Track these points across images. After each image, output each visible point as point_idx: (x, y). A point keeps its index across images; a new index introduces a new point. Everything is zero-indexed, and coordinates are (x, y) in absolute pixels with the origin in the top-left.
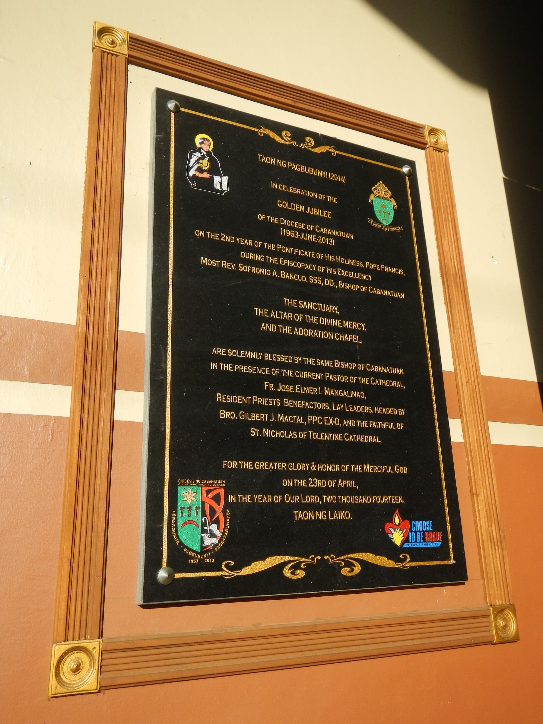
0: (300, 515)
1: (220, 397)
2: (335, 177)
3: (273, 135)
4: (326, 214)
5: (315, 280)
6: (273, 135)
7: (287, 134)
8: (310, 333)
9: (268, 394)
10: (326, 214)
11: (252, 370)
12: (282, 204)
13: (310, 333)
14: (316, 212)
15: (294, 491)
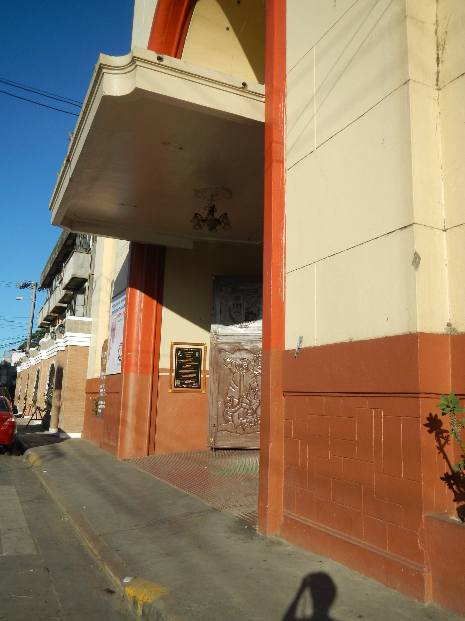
0: (186, 383)
1: (180, 374)
2: (192, 352)
3: (186, 350)
4: (191, 357)
5: (189, 363)
6: (186, 350)
7: (187, 349)
8: (188, 368)
9: (184, 373)
10: (191, 357)
11: (183, 371)
12: (186, 356)
13: (188, 368)
14: (190, 356)
15: (185, 381)
